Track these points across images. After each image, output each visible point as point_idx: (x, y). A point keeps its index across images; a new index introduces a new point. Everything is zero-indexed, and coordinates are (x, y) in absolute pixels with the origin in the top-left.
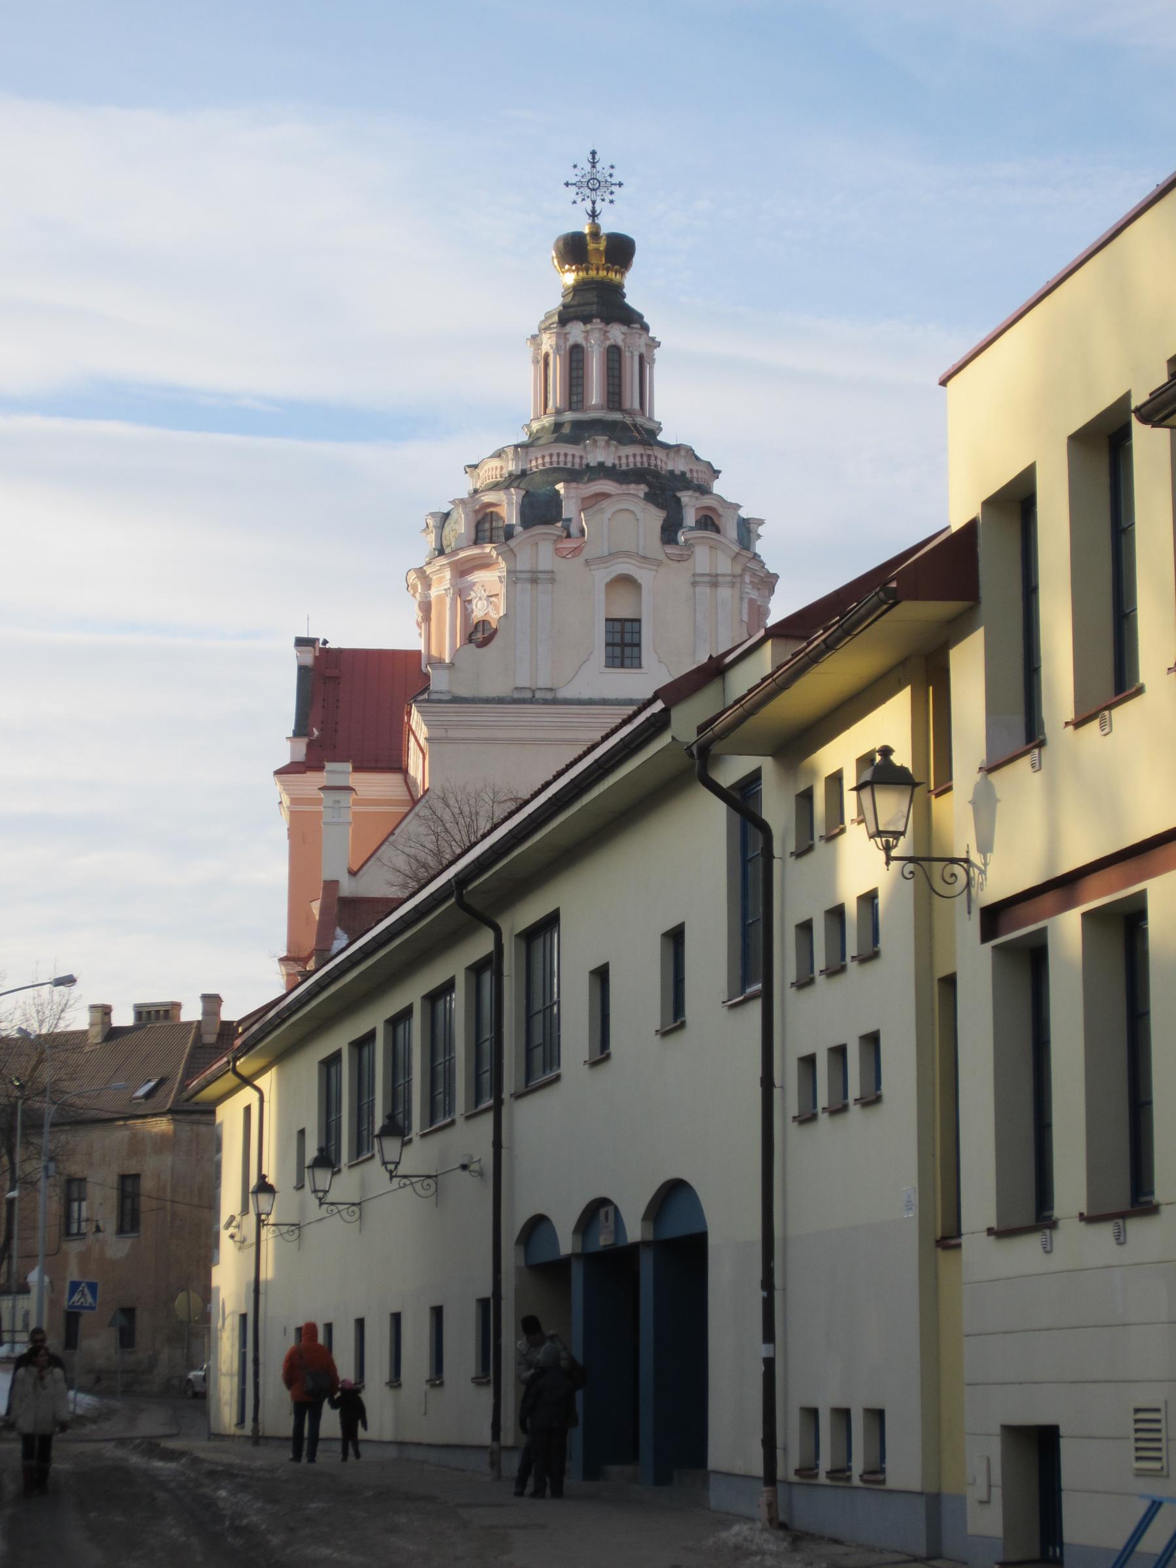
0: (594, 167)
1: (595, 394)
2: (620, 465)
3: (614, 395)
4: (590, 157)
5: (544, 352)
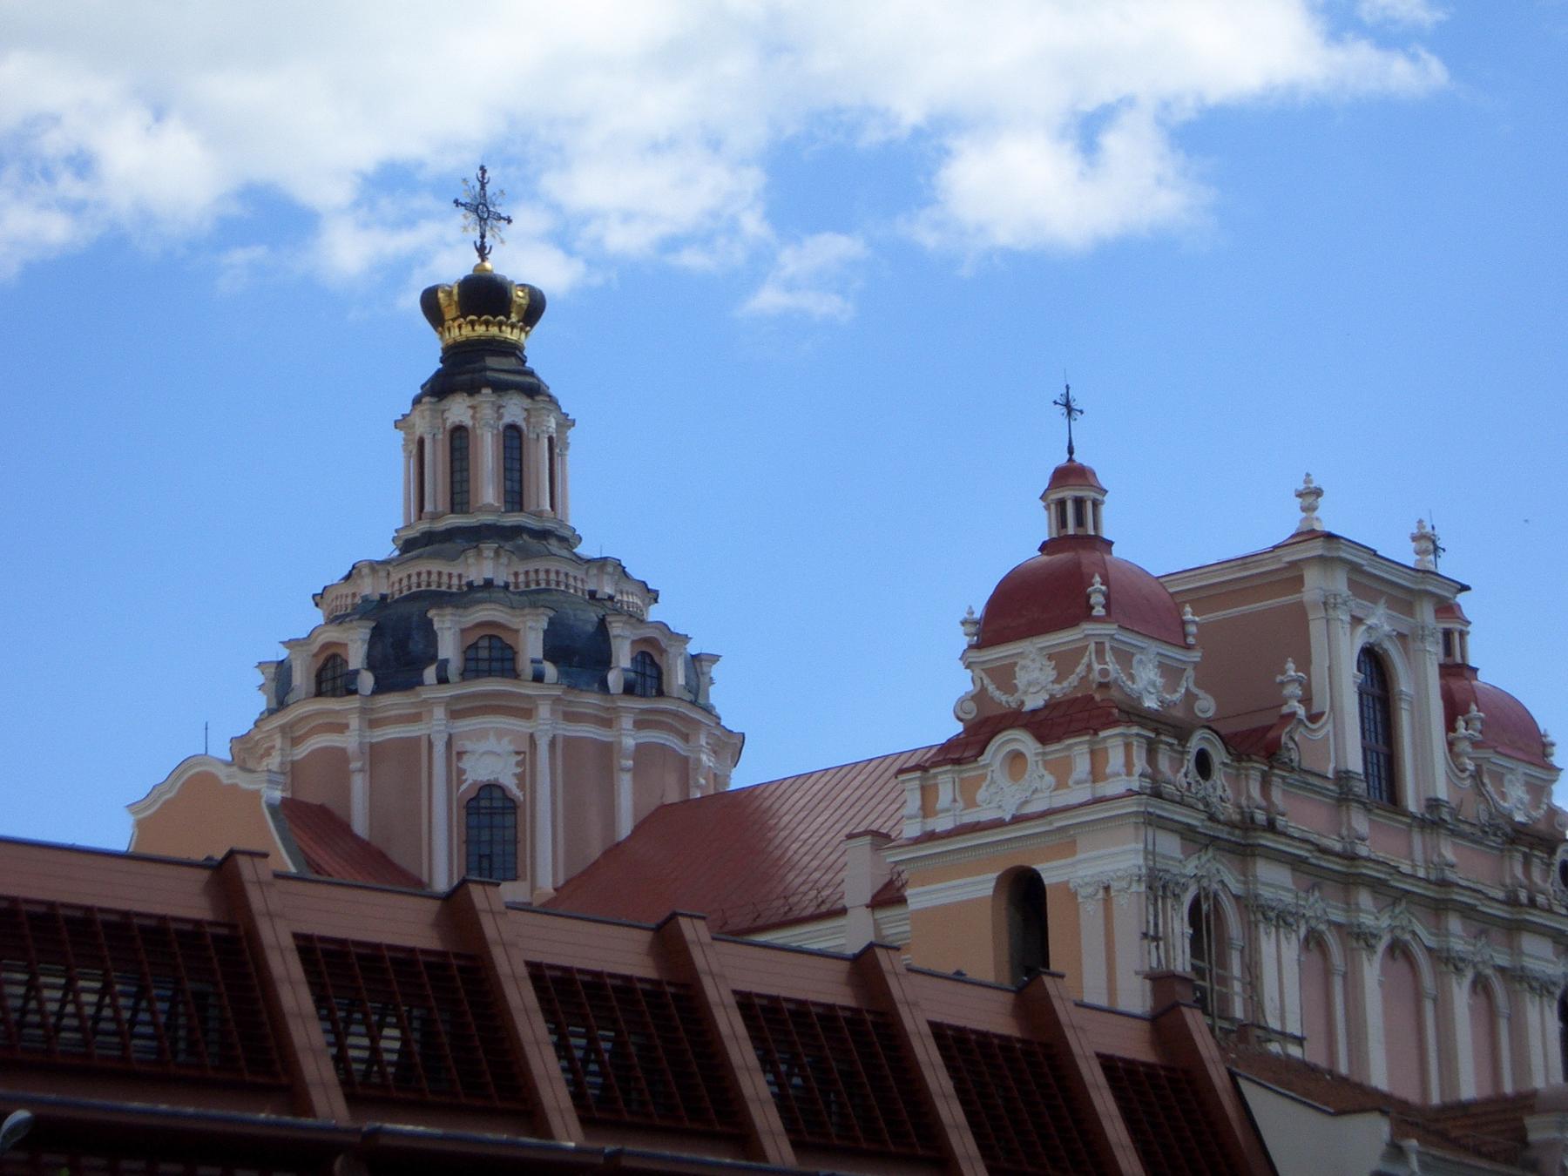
1: (488, 491)
2: (517, 585)
3: (515, 497)
4: (480, 175)
5: (417, 438)
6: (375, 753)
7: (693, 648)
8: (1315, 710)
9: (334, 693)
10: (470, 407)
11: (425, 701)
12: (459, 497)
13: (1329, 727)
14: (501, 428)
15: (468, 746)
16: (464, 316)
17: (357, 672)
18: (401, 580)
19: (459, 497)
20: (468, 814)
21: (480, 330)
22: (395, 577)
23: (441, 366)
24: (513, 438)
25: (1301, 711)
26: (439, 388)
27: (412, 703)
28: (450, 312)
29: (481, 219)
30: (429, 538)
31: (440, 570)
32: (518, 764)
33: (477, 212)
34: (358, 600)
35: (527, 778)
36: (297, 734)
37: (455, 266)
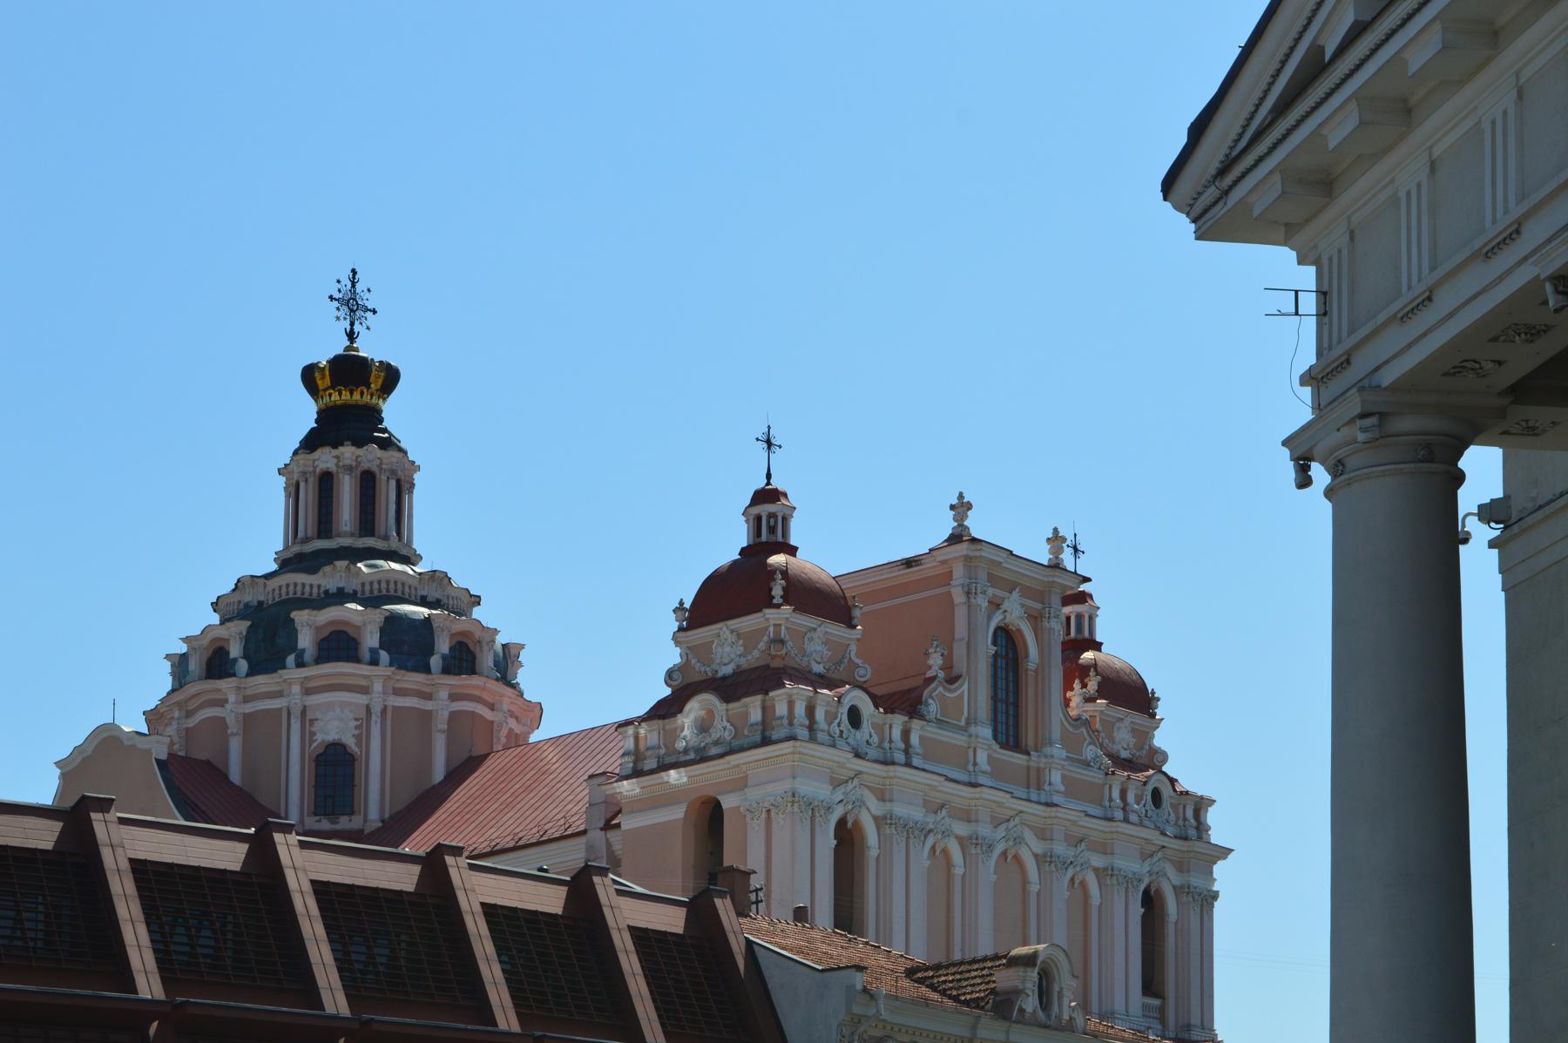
0: (353, 285)
2: (363, 591)
3: (367, 521)
4: (351, 276)
6: (248, 720)
8: (955, 671)
9: (220, 677)
10: (334, 457)
11: (285, 680)
12: (325, 525)
13: (965, 687)
14: (359, 475)
15: (318, 715)
16: (333, 387)
17: (235, 660)
18: (274, 590)
19: (325, 525)
20: (317, 766)
21: (346, 396)
22: (269, 588)
23: (316, 425)
24: (368, 482)
25: (941, 674)
26: (311, 443)
27: (277, 683)
28: (323, 382)
29: (352, 310)
30: (300, 557)
31: (304, 581)
32: (357, 727)
33: (348, 306)
34: (242, 606)
35: (363, 737)
36: (190, 708)
37: (327, 346)
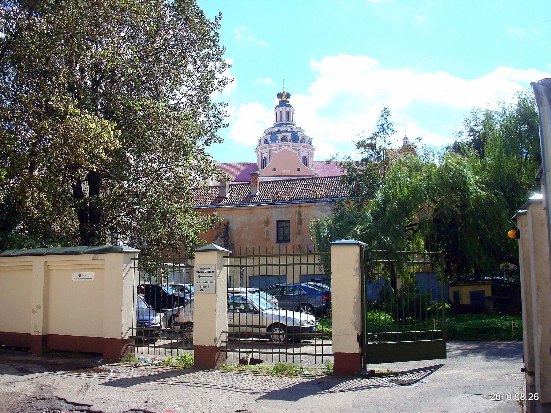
1: (284, 118)
3: (288, 119)
7: (309, 138)
12: (281, 120)
19: (281, 120)
26: (278, 107)
